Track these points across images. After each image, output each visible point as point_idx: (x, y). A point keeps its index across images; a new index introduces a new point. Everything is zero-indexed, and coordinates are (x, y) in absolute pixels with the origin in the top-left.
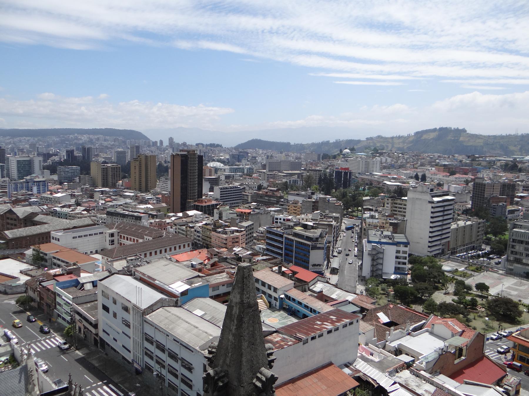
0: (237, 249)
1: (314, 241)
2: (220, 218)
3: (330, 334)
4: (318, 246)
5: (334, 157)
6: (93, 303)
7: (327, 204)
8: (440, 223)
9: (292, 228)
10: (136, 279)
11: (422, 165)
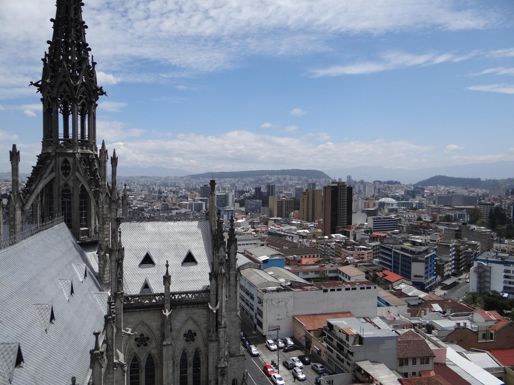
3: (348, 291)
4: (419, 259)
7: (471, 232)
9: (401, 243)
10: (245, 256)
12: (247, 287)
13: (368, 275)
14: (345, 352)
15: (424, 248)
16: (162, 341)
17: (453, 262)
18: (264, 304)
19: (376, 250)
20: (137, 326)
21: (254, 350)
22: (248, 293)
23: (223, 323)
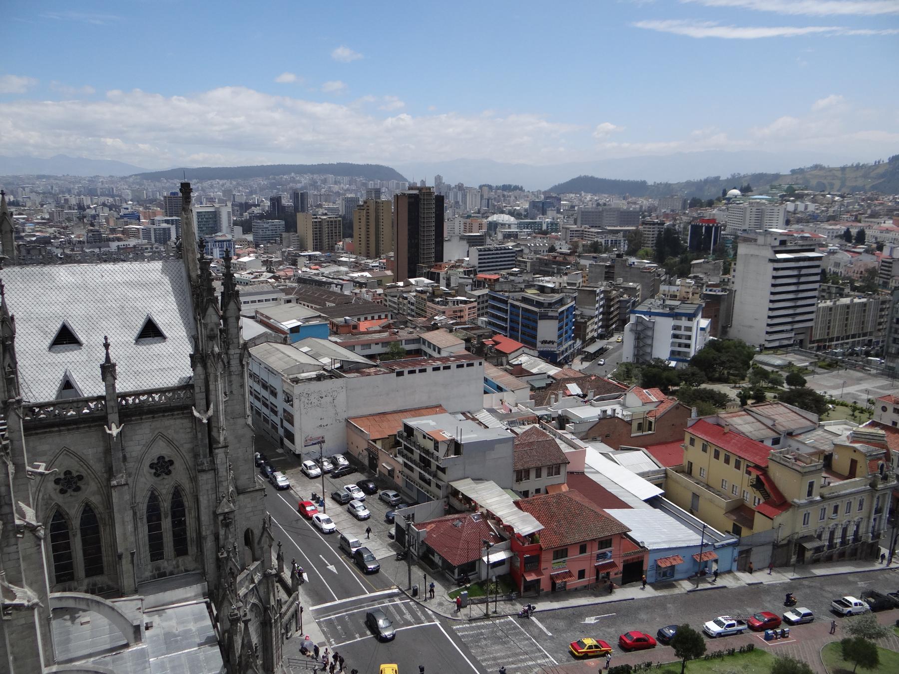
4: (550, 314)
5: (710, 204)
7: (628, 269)
9: (522, 290)
10: (257, 321)
11: (874, 215)
12: (264, 376)
13: (469, 344)
14: (433, 468)
15: (557, 297)
16: (109, 480)
17: (601, 317)
18: (296, 402)
19: (483, 302)
20: (56, 457)
21: (281, 480)
22: (265, 386)
23: (222, 439)
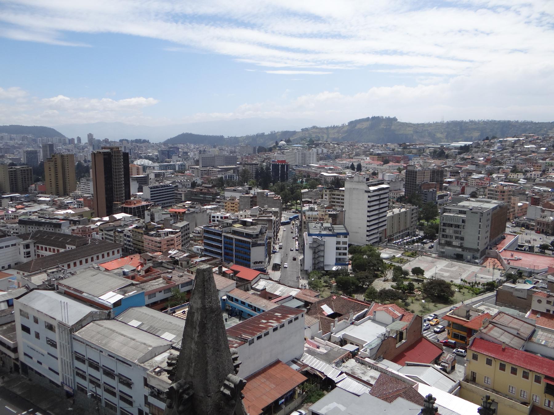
0: (172, 252)
1: (254, 238)
2: (152, 219)
3: (276, 332)
4: (259, 242)
5: (270, 150)
6: (9, 325)
7: (265, 198)
8: (377, 212)
9: (231, 225)
10: (60, 293)
11: (357, 155)
